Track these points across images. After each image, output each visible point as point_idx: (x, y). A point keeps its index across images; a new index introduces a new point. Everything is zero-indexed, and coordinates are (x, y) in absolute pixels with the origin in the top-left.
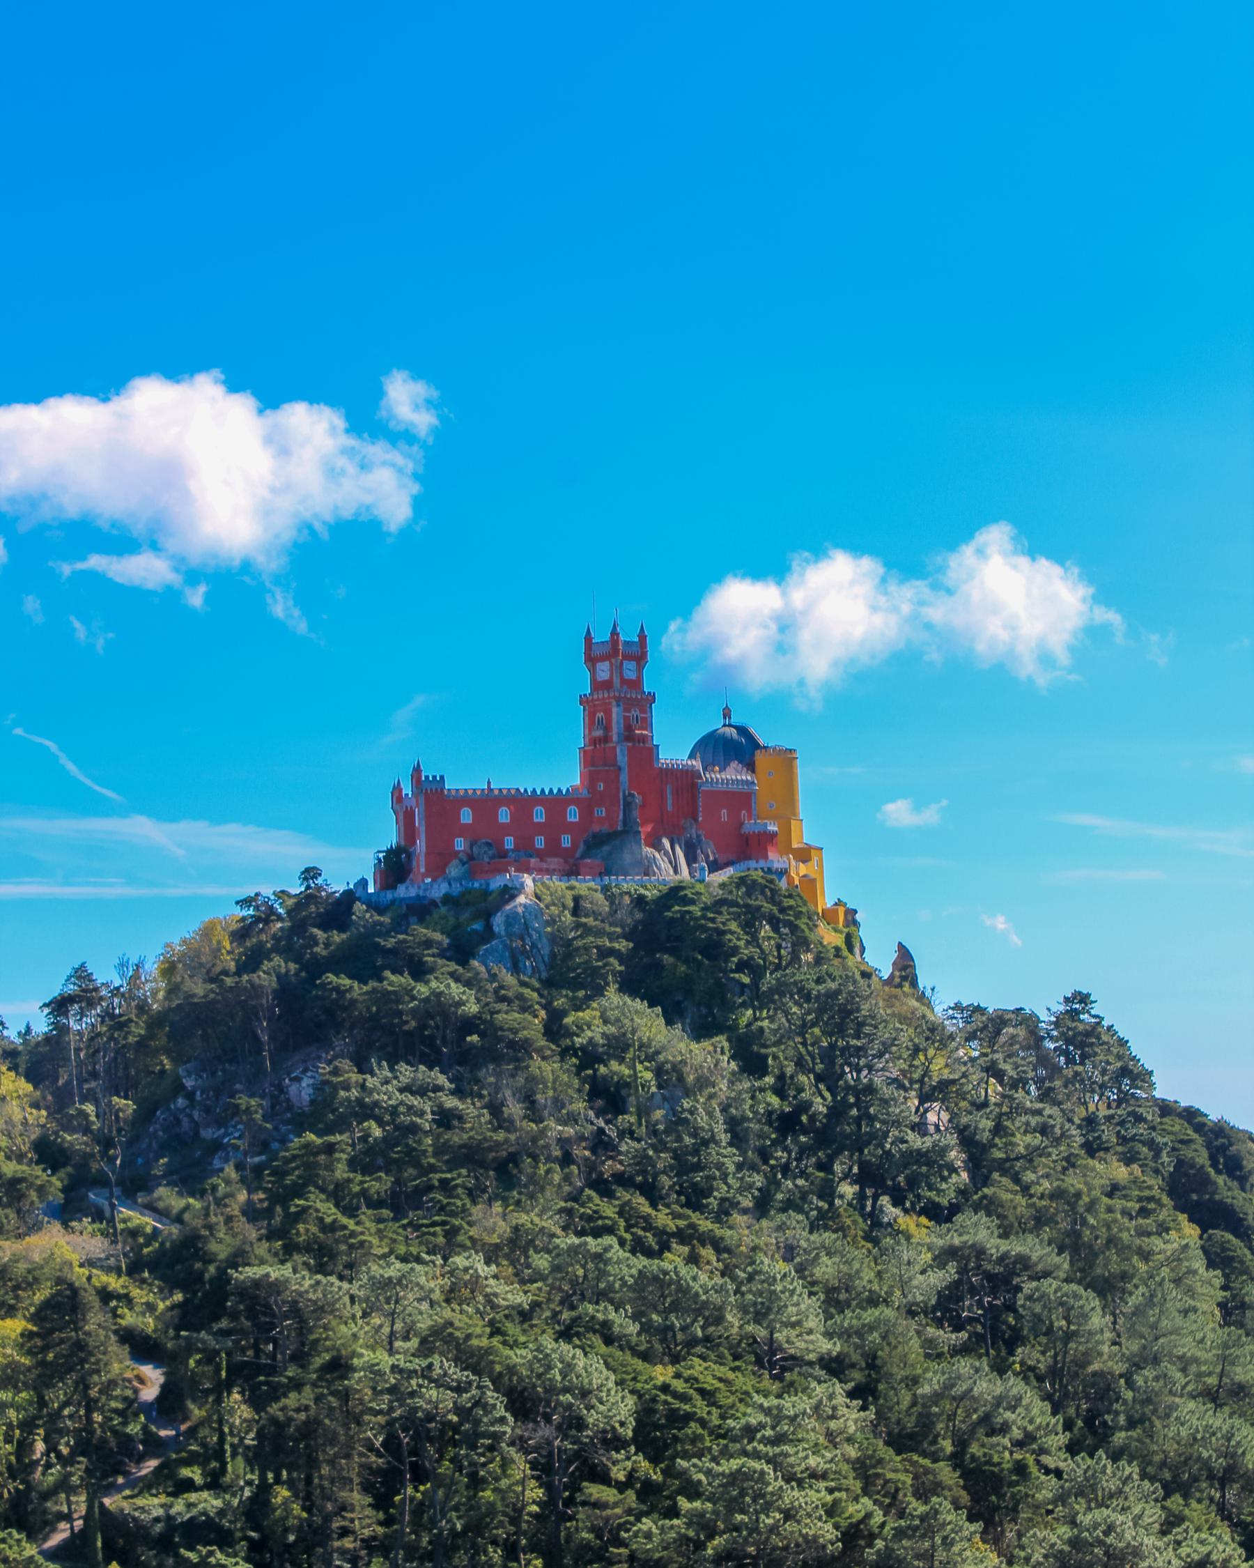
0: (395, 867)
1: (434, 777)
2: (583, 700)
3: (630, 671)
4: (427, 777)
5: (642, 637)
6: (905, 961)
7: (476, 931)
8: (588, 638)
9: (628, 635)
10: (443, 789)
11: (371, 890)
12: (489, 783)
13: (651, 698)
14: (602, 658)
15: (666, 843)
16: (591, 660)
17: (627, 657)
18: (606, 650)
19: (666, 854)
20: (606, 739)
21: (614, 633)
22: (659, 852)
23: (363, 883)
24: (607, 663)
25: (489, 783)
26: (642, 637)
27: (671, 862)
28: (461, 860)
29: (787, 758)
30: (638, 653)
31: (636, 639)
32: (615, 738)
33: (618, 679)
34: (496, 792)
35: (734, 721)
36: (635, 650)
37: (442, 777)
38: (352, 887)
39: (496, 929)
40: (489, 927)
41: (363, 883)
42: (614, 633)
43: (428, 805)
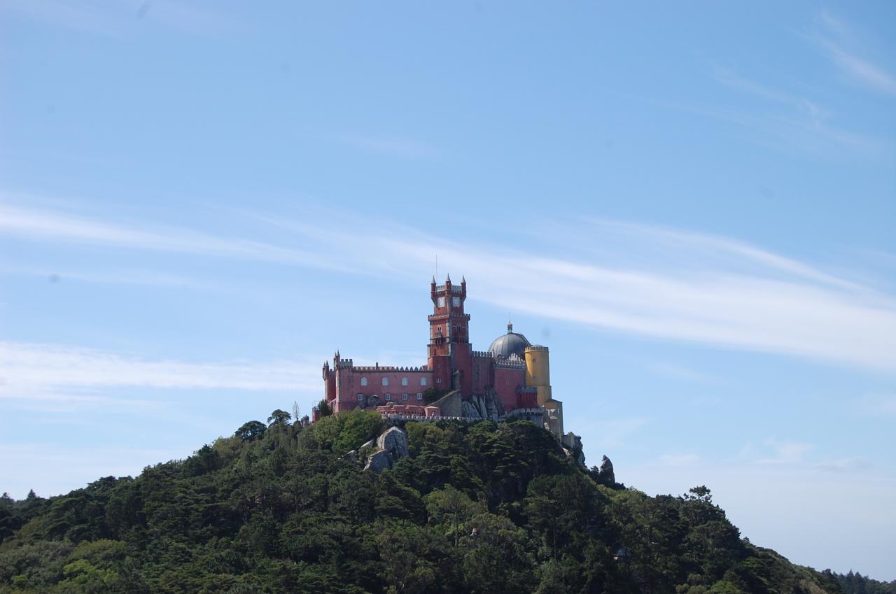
0: (323, 410)
1: (347, 360)
3: (456, 301)
4: (343, 360)
6: (608, 464)
8: (434, 285)
9: (456, 283)
10: (351, 366)
11: (311, 420)
12: (377, 364)
13: (468, 318)
14: (442, 294)
15: (475, 399)
16: (435, 296)
17: (456, 295)
20: (443, 339)
21: (449, 283)
23: (307, 418)
24: (443, 298)
25: (377, 364)
26: (464, 284)
29: (543, 352)
30: (462, 294)
31: (460, 285)
32: (448, 340)
33: (451, 306)
34: (381, 369)
35: (513, 332)
37: (351, 360)
38: (300, 420)
39: (379, 445)
40: (375, 444)
41: (307, 418)
42: (449, 283)
43: (341, 375)
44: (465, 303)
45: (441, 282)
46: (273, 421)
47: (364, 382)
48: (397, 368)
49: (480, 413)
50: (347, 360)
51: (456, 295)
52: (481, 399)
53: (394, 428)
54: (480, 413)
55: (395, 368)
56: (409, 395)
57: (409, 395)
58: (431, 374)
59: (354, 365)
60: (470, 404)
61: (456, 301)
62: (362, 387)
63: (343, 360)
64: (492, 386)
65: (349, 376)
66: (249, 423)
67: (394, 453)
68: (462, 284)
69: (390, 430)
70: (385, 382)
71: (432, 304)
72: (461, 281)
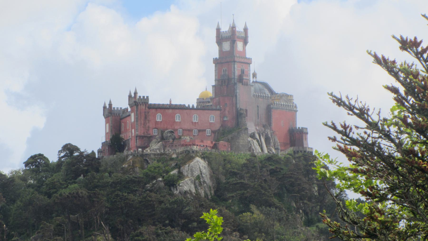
2: (216, 61)
5: (246, 30)
7: (174, 175)
8: (218, 30)
9: (240, 28)
10: (147, 103)
12: (170, 101)
17: (240, 38)
18: (229, 34)
19: (258, 141)
21: (233, 28)
22: (254, 139)
25: (170, 101)
26: (246, 30)
27: (259, 146)
28: (157, 140)
31: (242, 30)
36: (243, 35)
37: (147, 97)
42: (233, 28)
44: (248, 47)
45: (225, 28)
46: (62, 154)
47: (159, 118)
48: (189, 105)
49: (262, 150)
50: (144, 97)
51: (240, 38)
52: (262, 137)
53: (198, 159)
54: (262, 150)
55: (187, 106)
56: (199, 131)
57: (199, 131)
58: (218, 112)
59: (152, 101)
60: (254, 140)
61: (240, 45)
62: (156, 123)
63: (140, 97)
64: (270, 124)
65: (145, 112)
66: (35, 156)
67: (200, 182)
68: (244, 29)
69: (195, 161)
70: (178, 119)
71: (216, 48)
72: (243, 27)
